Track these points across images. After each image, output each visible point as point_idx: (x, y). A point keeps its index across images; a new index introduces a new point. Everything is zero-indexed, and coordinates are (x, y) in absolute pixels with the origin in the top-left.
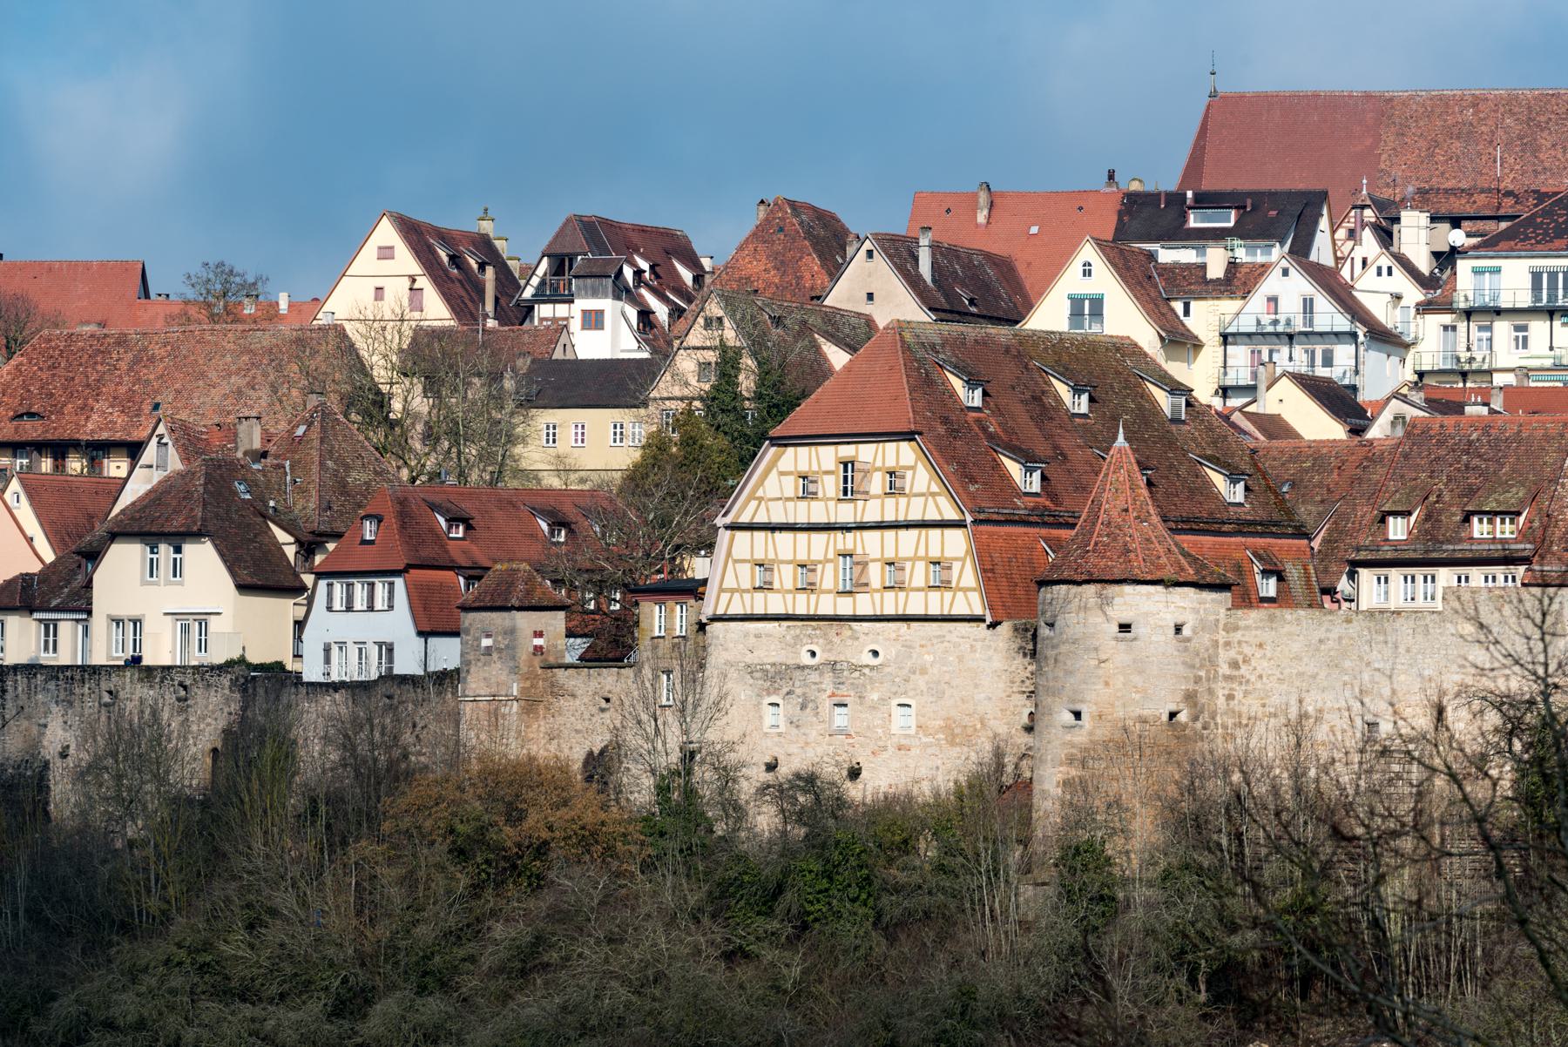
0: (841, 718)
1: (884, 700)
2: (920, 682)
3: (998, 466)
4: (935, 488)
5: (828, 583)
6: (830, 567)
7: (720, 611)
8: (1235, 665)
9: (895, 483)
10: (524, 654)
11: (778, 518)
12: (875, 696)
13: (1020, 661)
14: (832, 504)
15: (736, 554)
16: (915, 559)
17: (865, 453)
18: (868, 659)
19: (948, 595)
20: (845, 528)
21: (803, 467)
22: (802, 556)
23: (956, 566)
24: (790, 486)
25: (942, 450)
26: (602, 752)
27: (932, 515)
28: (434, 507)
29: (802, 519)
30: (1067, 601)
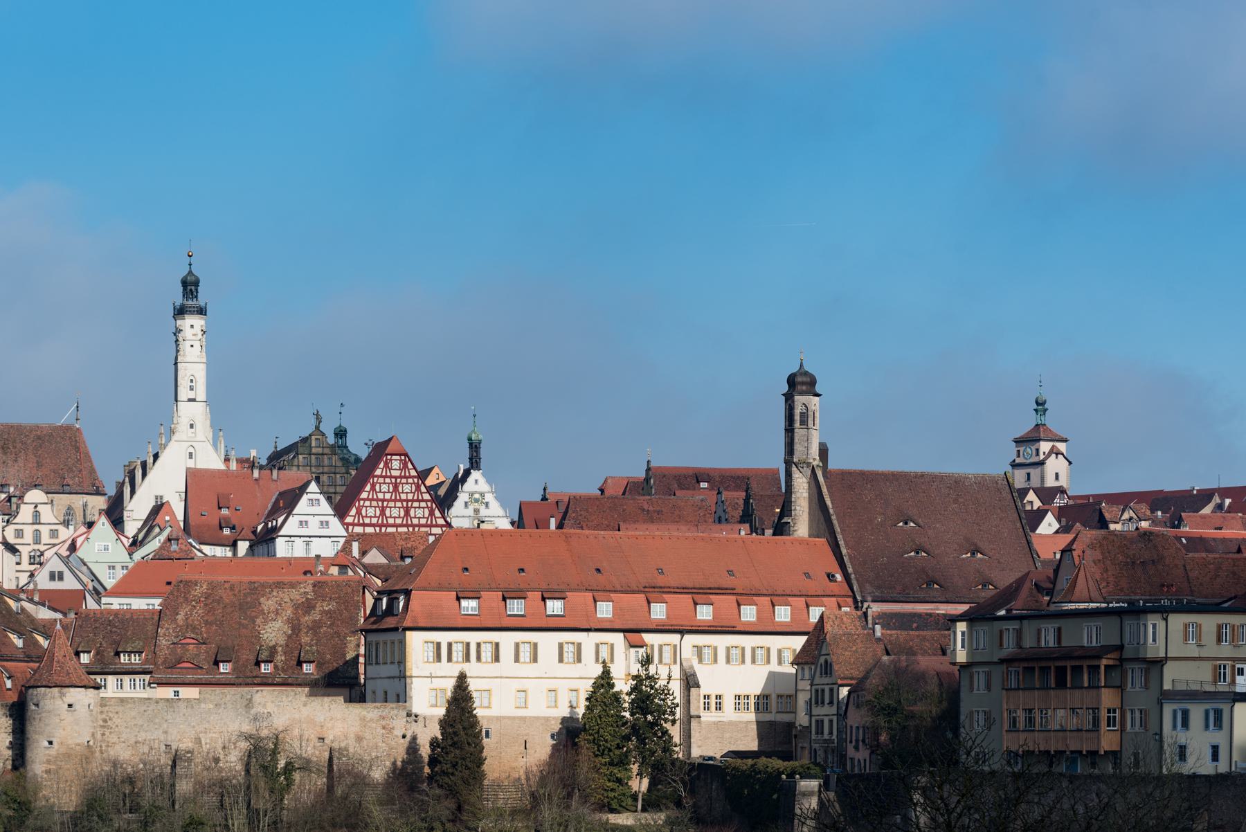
8: (105, 721)
30: (45, 694)
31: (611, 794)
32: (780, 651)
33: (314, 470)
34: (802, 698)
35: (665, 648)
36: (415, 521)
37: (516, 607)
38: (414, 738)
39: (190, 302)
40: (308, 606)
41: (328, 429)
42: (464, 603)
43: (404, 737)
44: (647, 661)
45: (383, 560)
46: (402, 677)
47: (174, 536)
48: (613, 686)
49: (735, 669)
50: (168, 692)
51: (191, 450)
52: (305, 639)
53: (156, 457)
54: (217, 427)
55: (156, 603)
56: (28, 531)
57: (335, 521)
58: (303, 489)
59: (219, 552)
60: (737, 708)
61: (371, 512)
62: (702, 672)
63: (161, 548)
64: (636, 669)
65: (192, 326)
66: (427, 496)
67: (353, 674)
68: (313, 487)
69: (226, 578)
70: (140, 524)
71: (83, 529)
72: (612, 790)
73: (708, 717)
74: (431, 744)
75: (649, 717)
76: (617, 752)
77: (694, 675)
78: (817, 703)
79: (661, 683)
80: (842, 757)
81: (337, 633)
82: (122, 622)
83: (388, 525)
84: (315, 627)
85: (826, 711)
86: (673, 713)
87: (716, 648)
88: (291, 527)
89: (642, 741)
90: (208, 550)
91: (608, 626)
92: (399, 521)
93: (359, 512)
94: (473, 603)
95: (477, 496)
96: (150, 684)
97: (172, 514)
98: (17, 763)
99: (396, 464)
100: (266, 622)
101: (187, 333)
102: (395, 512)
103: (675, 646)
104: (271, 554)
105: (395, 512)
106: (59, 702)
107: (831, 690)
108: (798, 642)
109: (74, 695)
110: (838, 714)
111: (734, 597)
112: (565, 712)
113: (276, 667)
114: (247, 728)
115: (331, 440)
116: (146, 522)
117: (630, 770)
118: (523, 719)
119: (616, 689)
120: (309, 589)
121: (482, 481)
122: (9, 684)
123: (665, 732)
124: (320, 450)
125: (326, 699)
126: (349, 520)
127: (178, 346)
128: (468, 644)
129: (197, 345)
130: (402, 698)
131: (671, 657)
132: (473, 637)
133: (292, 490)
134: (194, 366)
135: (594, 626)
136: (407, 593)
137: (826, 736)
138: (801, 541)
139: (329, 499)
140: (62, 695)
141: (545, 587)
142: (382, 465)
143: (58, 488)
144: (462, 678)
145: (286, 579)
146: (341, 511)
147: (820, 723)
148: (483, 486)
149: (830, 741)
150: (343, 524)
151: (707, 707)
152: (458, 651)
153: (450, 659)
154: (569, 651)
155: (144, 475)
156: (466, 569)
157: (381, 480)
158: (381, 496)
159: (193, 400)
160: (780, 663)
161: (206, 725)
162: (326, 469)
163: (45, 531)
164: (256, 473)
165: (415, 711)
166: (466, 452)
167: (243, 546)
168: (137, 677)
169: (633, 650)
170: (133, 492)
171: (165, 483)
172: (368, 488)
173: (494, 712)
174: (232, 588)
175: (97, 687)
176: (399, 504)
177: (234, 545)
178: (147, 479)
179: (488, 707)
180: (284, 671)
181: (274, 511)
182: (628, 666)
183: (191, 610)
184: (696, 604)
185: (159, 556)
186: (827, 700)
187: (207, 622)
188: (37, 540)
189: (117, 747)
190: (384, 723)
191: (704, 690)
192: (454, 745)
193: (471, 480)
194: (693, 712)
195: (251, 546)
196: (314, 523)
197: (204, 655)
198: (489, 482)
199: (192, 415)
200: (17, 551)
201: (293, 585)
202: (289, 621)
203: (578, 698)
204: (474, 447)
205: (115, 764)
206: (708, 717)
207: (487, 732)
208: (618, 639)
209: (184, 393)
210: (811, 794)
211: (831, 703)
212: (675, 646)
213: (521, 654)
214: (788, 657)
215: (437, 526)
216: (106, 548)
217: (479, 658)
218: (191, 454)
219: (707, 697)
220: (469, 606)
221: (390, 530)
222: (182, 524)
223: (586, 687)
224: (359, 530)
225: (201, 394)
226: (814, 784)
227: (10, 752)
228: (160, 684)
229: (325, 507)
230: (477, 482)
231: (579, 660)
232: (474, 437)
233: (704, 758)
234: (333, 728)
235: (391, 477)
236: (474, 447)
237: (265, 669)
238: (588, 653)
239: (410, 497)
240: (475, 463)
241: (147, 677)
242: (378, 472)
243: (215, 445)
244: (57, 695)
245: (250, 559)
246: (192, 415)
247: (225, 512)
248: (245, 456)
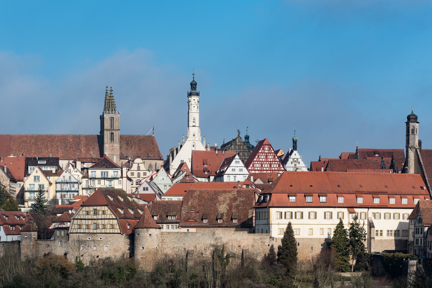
0: (95, 248)
1: (103, 246)
2: (109, 243)
3: (118, 210)
4: (111, 213)
5: (92, 228)
6: (92, 225)
7: (71, 232)
8: (163, 240)
9: (104, 213)
10: (33, 238)
11: (82, 217)
13: (127, 240)
16: (108, 224)
17: (98, 208)
18: (99, 239)
19: (114, 230)
20: (95, 219)
21: (87, 210)
22: (87, 223)
23: (115, 225)
24: (84, 213)
25: (111, 207)
26: (48, 254)
27: (111, 217)
28: (3, 215)
29: (87, 218)
31: (343, 266)
32: (403, 215)
33: (237, 151)
34: (411, 231)
35: (362, 214)
36: (273, 169)
37: (309, 199)
38: (272, 246)
39: (193, 91)
40: (235, 199)
41: (243, 136)
42: (291, 198)
43: (269, 245)
44: (356, 218)
45: (262, 183)
46: (268, 224)
47: (187, 174)
48: (343, 227)
49: (387, 221)
50: (185, 230)
51: (194, 144)
52: (234, 211)
53: (181, 146)
54: (203, 135)
55: (181, 198)
56: (136, 173)
57: (245, 169)
58: (233, 158)
59: (203, 180)
60: (388, 235)
61: (258, 165)
62: (376, 222)
63: (183, 179)
64: (352, 221)
65: (194, 100)
66: (277, 160)
67: (251, 223)
68: (237, 157)
69: (206, 189)
70: (175, 170)
71: (155, 172)
72: (343, 264)
73: (377, 238)
74: (278, 248)
75: (356, 238)
76: (345, 251)
77: (373, 223)
78: (416, 233)
79: (361, 226)
80: (425, 252)
81: (245, 209)
82: (169, 205)
83: (264, 170)
84: (237, 207)
85: (419, 236)
86: (365, 237)
87: (380, 214)
88: (229, 171)
89: (354, 246)
90: (199, 179)
91: (342, 206)
92: (267, 169)
93: (253, 166)
94: (294, 198)
95: (295, 160)
96: (178, 227)
97: (187, 167)
98: (131, 255)
99: (267, 148)
100: (220, 205)
101: (192, 102)
102: (266, 166)
103: (366, 213)
104: (222, 181)
105: (266, 166)
106: (146, 233)
107: (422, 228)
108: (410, 211)
109: (152, 231)
110: (424, 237)
111: (387, 195)
112: (326, 237)
113: (223, 221)
114: (213, 242)
115: (244, 140)
116: (177, 169)
117: (349, 257)
118: (311, 239)
119: (345, 228)
120: (235, 193)
121: (297, 154)
122: (128, 227)
123: (362, 244)
124: (239, 144)
125: (241, 232)
126: (250, 168)
127: (189, 107)
128: (292, 212)
129: (196, 106)
130: (268, 232)
131: (364, 216)
132: (294, 210)
133: (230, 158)
134: (195, 114)
135: (337, 206)
136: (270, 194)
137: (419, 245)
138: (412, 175)
139: (243, 161)
140: (147, 231)
141: (319, 192)
142: (261, 149)
143: (146, 158)
144: (290, 224)
145: (227, 189)
146: (247, 165)
147: (417, 240)
148: (298, 156)
149: (421, 246)
150: (248, 170)
151: (377, 235)
152: (288, 215)
153: (285, 218)
154: (328, 215)
155: (177, 153)
156: (291, 186)
157: (261, 154)
158: (261, 160)
159: (194, 126)
160: (403, 219)
161: (199, 241)
162: (242, 150)
163: (142, 173)
164: (217, 152)
165: (273, 236)
166: (292, 144)
167: (212, 178)
168: (174, 225)
169: (351, 214)
170: (173, 159)
171: (184, 156)
172: (257, 157)
173: (301, 236)
174: (208, 193)
175: (160, 228)
176: (268, 163)
177: (209, 178)
178: (178, 154)
179: (299, 235)
180: (226, 222)
181: (223, 166)
182: (349, 220)
183: (193, 201)
184: (373, 198)
185: (182, 182)
186: (420, 232)
187: (199, 205)
188: (139, 176)
189: (167, 249)
190: (262, 240)
191: (376, 229)
192: (286, 248)
193: (293, 154)
194: (372, 236)
195: (215, 178)
196: (237, 169)
197: (198, 217)
198: (300, 154)
199: (194, 131)
200: (132, 180)
201: (230, 192)
202: (228, 204)
203: (331, 231)
204: (295, 142)
205: (166, 255)
206: (377, 238)
207: (298, 244)
208: (345, 210)
209: (191, 124)
210: (414, 265)
211: (421, 233)
212: (366, 213)
213: (311, 216)
214: (406, 216)
215: (281, 170)
216: (163, 179)
217: (296, 218)
218: (194, 146)
219: (377, 231)
220: (292, 199)
221: (264, 172)
222: (190, 170)
223: (334, 227)
224: (253, 172)
225: (197, 124)
226: (415, 262)
227: (129, 251)
228: (182, 227)
229: (241, 164)
230: (295, 155)
231: (332, 218)
232: (294, 139)
233: (376, 253)
234: (243, 242)
235: (265, 153)
236: (295, 142)
237: (220, 221)
238: (335, 216)
239: (272, 160)
240: (295, 148)
241: (178, 225)
242: (260, 151)
243: (202, 142)
244: (146, 231)
245: (214, 183)
246: (194, 131)
247: (205, 166)
248: (213, 146)
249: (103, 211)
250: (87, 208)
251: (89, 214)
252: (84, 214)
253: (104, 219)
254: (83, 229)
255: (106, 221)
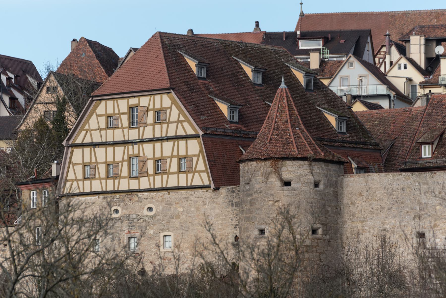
2: (176, 223)
4: (182, 118)
9: (159, 117)
11: (97, 139)
12: (151, 232)
14: (126, 130)
15: (74, 160)
16: (172, 157)
17: (144, 101)
19: (190, 175)
20: (133, 143)
21: (110, 111)
23: (195, 159)
24: (103, 122)
27: (181, 133)
29: (110, 139)
249: (157, 112)
250: (110, 103)
251: (117, 127)
252: (103, 125)
253: (161, 139)
254: (100, 179)
255: (168, 146)
